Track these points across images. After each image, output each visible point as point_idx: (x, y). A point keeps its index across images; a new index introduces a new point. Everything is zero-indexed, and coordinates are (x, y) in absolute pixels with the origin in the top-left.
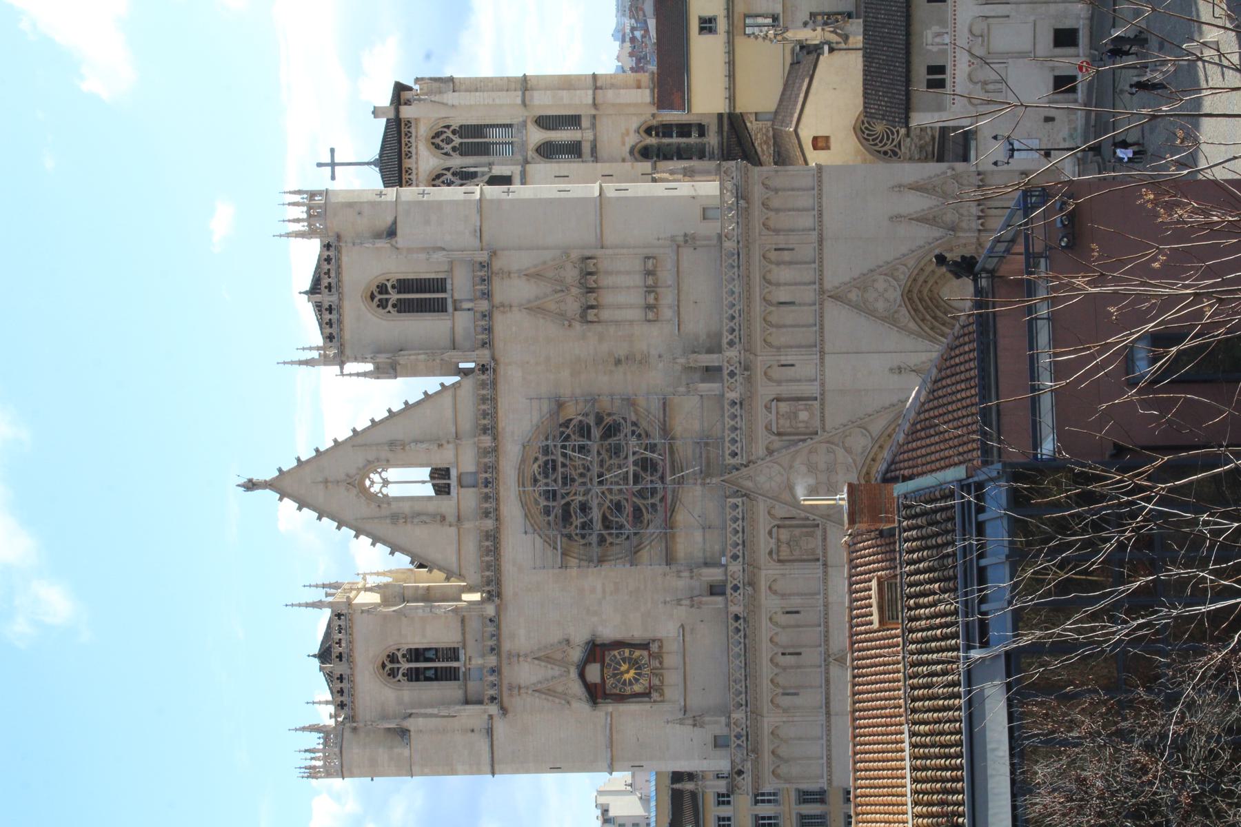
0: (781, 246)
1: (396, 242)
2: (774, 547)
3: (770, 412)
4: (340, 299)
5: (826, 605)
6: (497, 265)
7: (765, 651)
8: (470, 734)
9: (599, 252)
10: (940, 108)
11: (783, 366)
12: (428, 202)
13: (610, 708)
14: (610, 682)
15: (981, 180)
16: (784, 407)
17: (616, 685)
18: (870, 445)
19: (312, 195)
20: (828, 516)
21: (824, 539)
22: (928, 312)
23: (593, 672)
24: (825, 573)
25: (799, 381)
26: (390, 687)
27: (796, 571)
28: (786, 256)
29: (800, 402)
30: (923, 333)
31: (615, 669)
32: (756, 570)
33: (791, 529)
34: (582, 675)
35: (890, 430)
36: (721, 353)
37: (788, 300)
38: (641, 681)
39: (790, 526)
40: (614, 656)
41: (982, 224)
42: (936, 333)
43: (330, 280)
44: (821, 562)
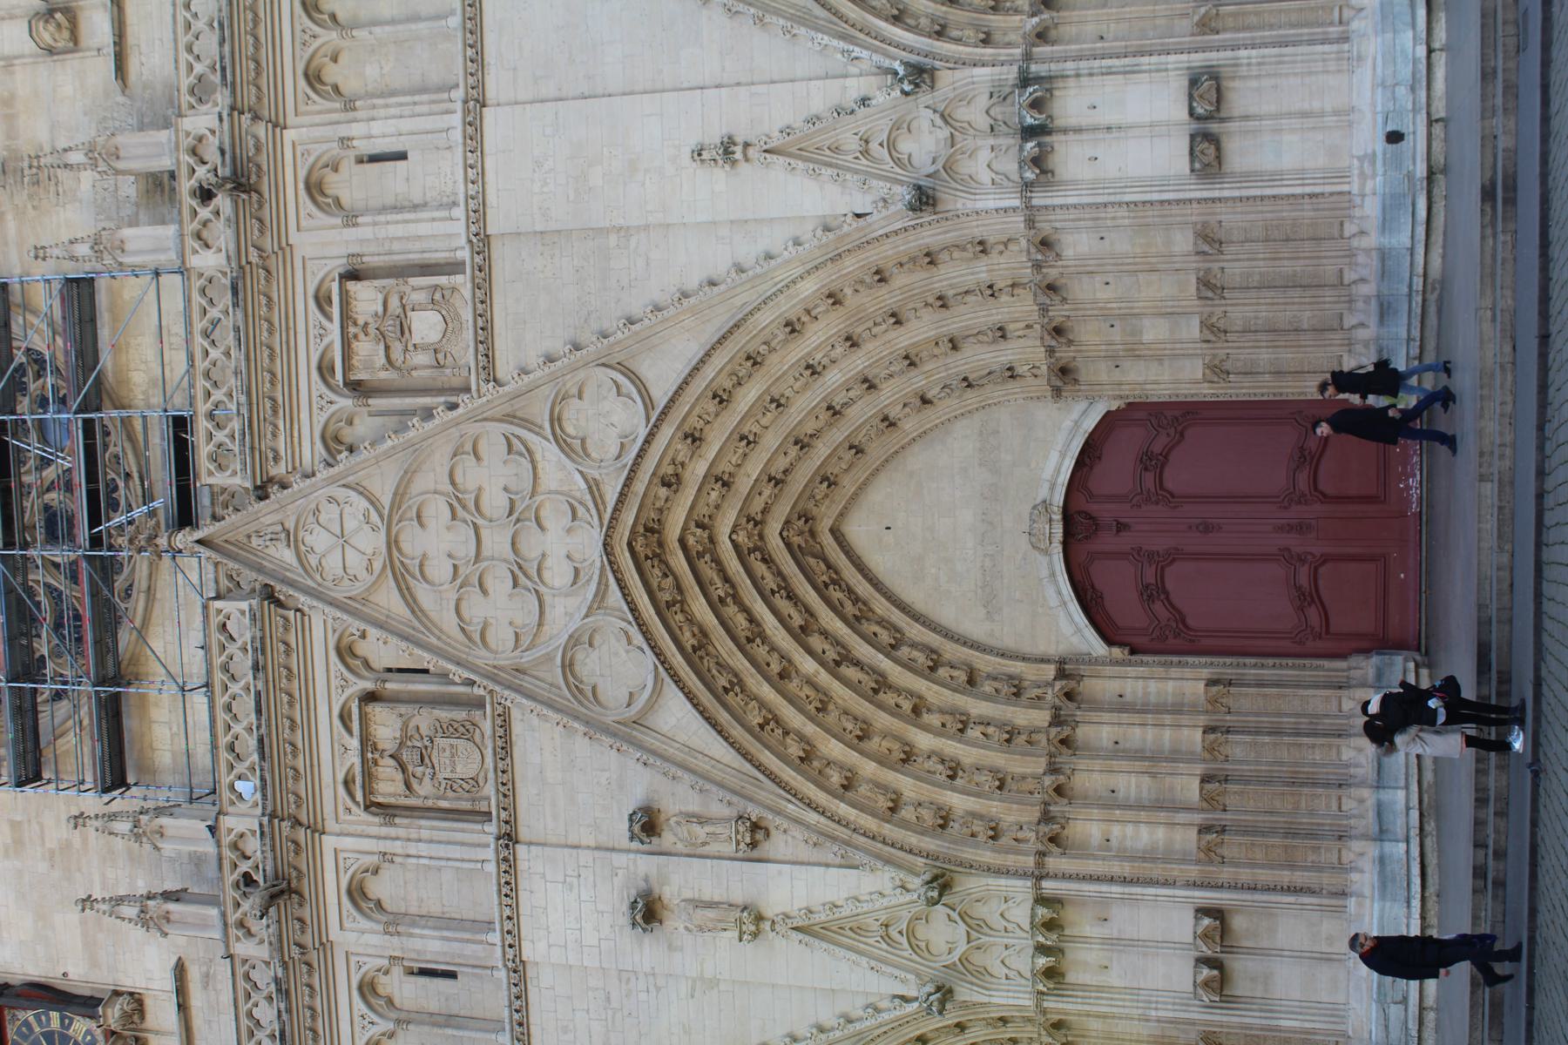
2: (357, 761)
3: (329, 318)
5: (518, 970)
11: (374, 159)
16: (366, 298)
18: (643, 433)
21: (505, 748)
24: (508, 865)
25: (423, 206)
27: (423, 849)
32: (301, 834)
33: (403, 709)
36: (167, 125)
40: (26, 1023)
42: (873, 11)
44: (492, 828)
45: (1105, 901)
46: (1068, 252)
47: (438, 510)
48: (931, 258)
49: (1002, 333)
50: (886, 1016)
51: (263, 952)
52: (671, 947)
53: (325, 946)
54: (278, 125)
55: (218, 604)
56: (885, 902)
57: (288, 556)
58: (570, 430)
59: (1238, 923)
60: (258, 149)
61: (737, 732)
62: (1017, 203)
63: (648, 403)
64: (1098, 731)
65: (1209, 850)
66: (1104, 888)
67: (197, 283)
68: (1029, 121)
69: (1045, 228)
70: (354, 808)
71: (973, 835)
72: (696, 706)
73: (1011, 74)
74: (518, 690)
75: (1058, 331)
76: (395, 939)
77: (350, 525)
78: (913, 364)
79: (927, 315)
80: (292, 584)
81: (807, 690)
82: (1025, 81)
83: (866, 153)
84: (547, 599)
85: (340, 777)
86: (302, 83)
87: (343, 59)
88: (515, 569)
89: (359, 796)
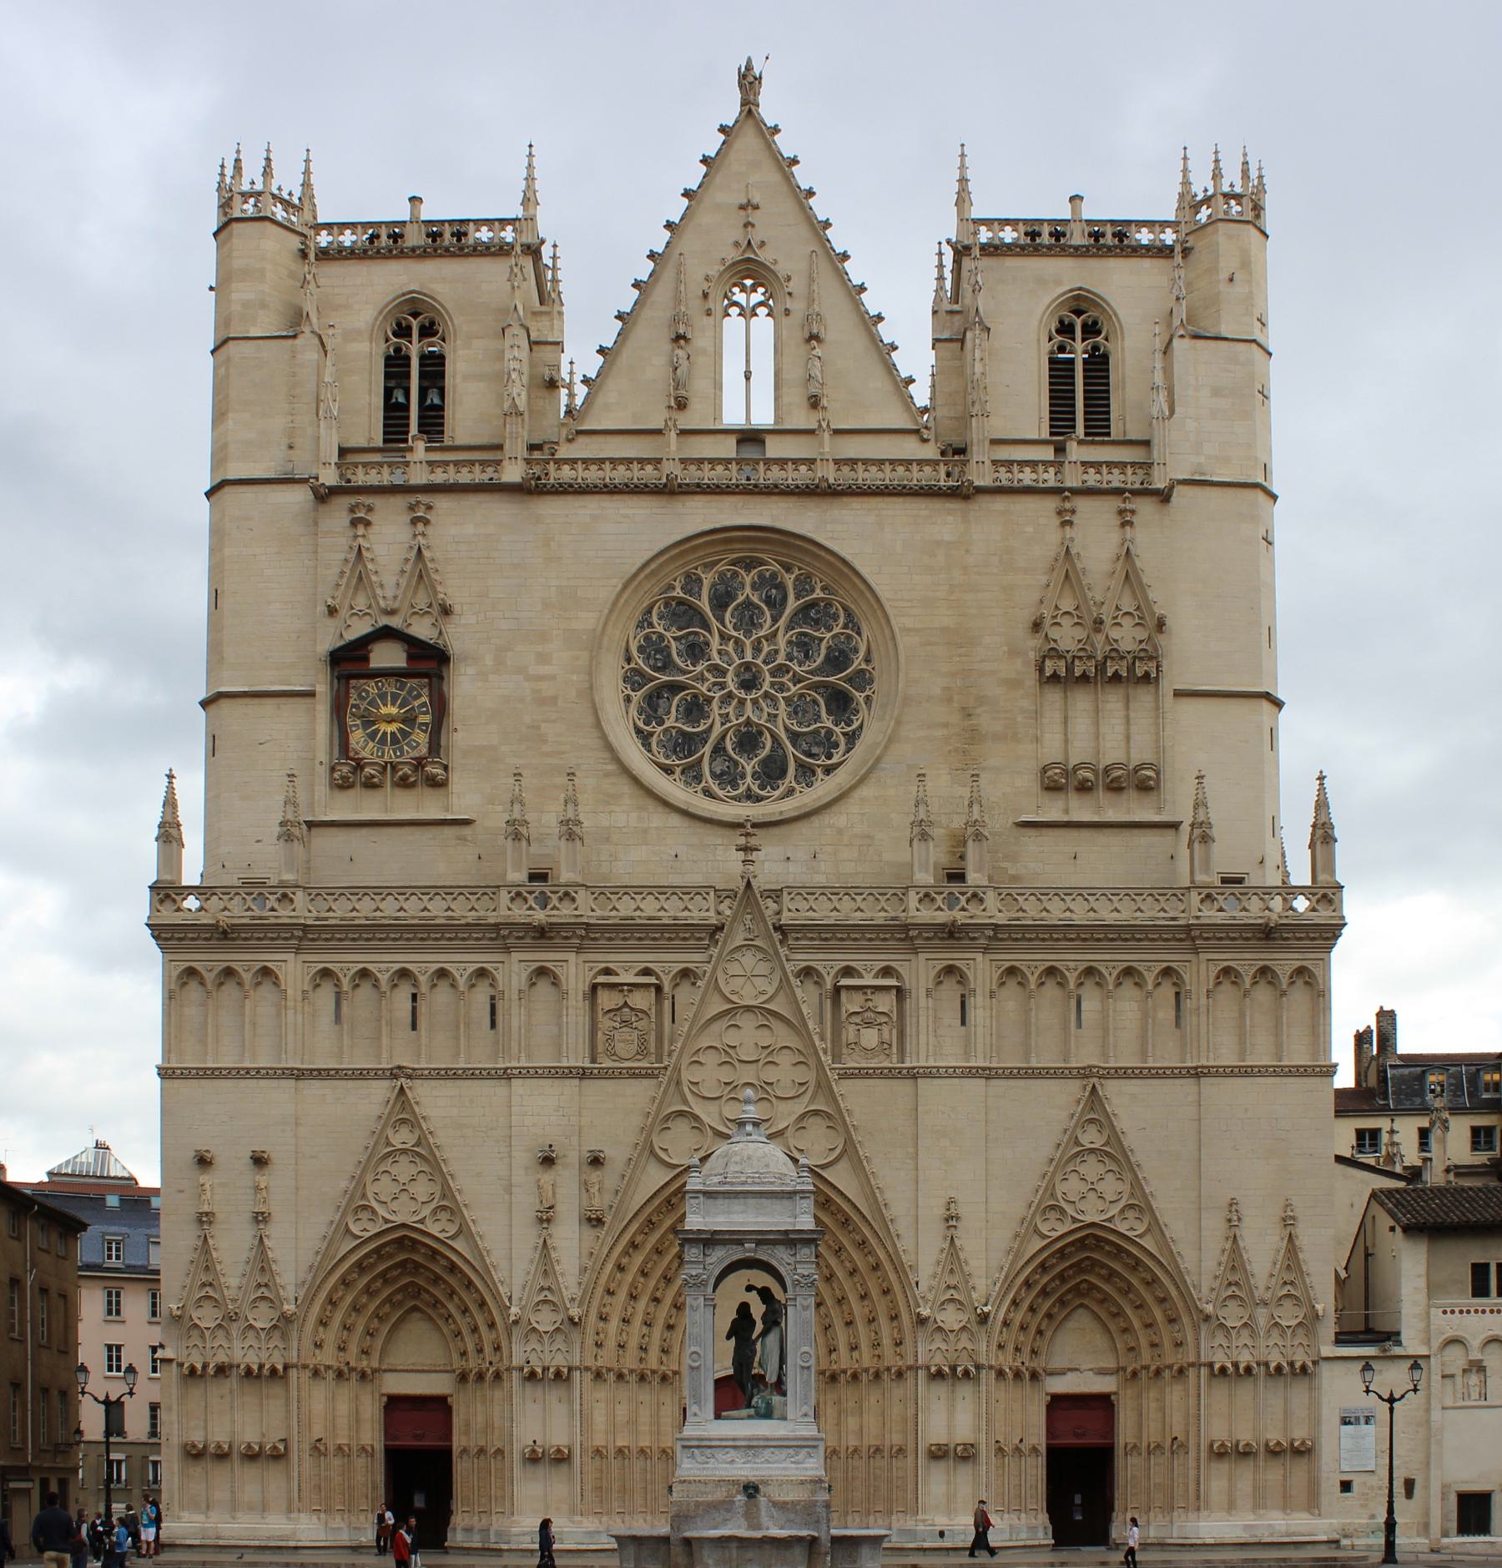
0: (1188, 1004)
1: (1182, 336)
3: (876, 976)
4: (1076, 248)
5: (506, 1075)
6: (1145, 508)
7: (422, 963)
8: (284, 447)
9: (1168, 685)
10: (1433, 1289)
12: (1254, 396)
13: (323, 689)
14: (371, 687)
15: (1304, 1368)
16: (885, 1003)
17: (364, 699)
19: (1258, 209)
20: (678, 1083)
21: (634, 1074)
22: (1053, 1279)
23: (387, 656)
26: (376, 319)
28: (1166, 1014)
29: (894, 1032)
30: (1021, 1263)
31: (395, 697)
34: (386, 634)
35: (839, 1200)
37: (1083, 1017)
38: (371, 744)
39: (659, 1013)
40: (419, 696)
41: (1223, 1370)
42: (1020, 1289)
43: (1109, 236)
45: (570, 1402)
46: (894, 1384)
47: (765, 1038)
48: (894, 1318)
49: (854, 1348)
50: (500, 1288)
51: (504, 912)
52: (527, 1168)
53: (507, 950)
54: (986, 950)
55: (712, 893)
56: (563, 1290)
57: (739, 942)
58: (811, 1120)
59: (564, 1468)
60: (974, 939)
61: (649, 1209)
62: (920, 1362)
63: (823, 1167)
64: (645, 1395)
65: (598, 1451)
66: (578, 1401)
67: (899, 892)
68: (959, 1369)
69: (909, 1374)
70: (592, 973)
71: (598, 1334)
72: (662, 1187)
73: (983, 1360)
74: (669, 1083)
75: (855, 1376)
76: (515, 996)
77: (758, 981)
78: (839, 1301)
79: (866, 1310)
80: (725, 942)
81: (667, 1243)
82: (978, 1367)
83: (949, 1287)
84: (717, 1102)
85: (610, 965)
86: (1008, 964)
87: (1019, 989)
88: (735, 1084)
89: (601, 979)
